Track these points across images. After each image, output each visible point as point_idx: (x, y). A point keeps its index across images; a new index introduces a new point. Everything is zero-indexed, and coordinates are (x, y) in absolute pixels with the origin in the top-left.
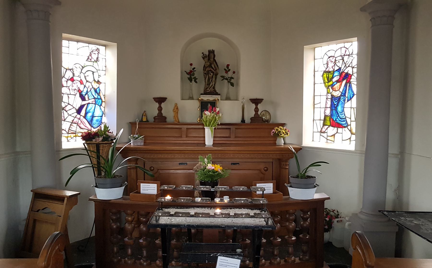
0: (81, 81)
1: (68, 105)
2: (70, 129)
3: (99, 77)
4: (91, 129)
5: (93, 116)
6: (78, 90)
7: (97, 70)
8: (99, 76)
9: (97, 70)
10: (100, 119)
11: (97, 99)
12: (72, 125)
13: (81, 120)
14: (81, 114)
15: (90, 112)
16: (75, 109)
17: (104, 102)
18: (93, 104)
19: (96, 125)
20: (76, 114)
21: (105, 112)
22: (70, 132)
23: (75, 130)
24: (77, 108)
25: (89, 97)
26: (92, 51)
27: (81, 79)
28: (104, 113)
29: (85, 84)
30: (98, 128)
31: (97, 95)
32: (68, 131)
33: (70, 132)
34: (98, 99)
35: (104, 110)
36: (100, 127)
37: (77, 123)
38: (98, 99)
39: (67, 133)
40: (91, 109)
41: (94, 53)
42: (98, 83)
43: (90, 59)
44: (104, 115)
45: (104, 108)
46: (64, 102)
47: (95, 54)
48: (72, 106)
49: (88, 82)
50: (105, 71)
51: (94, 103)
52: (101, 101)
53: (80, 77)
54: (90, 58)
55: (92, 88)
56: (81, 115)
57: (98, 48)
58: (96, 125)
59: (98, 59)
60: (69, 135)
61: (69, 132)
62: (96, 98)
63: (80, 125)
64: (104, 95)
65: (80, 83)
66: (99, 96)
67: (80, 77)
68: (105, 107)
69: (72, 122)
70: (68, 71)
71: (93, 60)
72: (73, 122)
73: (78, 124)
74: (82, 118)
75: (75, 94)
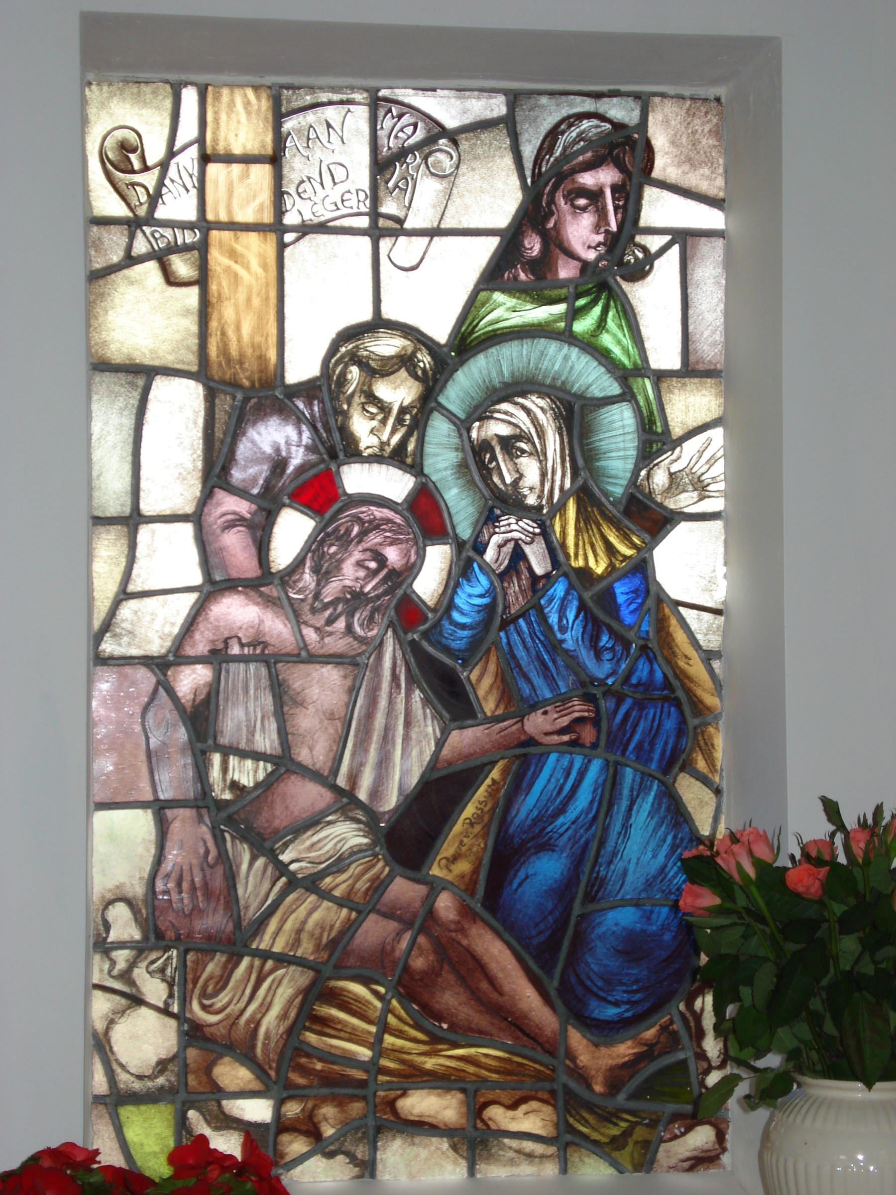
2: (311, 1038)
10: (667, 937)
14: (436, 871)
16: (360, 815)
19: (619, 996)
20: (380, 868)
24: (391, 801)
40: (562, 810)
41: (583, 192)
47: (595, 196)
54: (533, 245)
56: (435, 887)
60: (293, 1109)
67: (416, 468)
71: (566, 271)
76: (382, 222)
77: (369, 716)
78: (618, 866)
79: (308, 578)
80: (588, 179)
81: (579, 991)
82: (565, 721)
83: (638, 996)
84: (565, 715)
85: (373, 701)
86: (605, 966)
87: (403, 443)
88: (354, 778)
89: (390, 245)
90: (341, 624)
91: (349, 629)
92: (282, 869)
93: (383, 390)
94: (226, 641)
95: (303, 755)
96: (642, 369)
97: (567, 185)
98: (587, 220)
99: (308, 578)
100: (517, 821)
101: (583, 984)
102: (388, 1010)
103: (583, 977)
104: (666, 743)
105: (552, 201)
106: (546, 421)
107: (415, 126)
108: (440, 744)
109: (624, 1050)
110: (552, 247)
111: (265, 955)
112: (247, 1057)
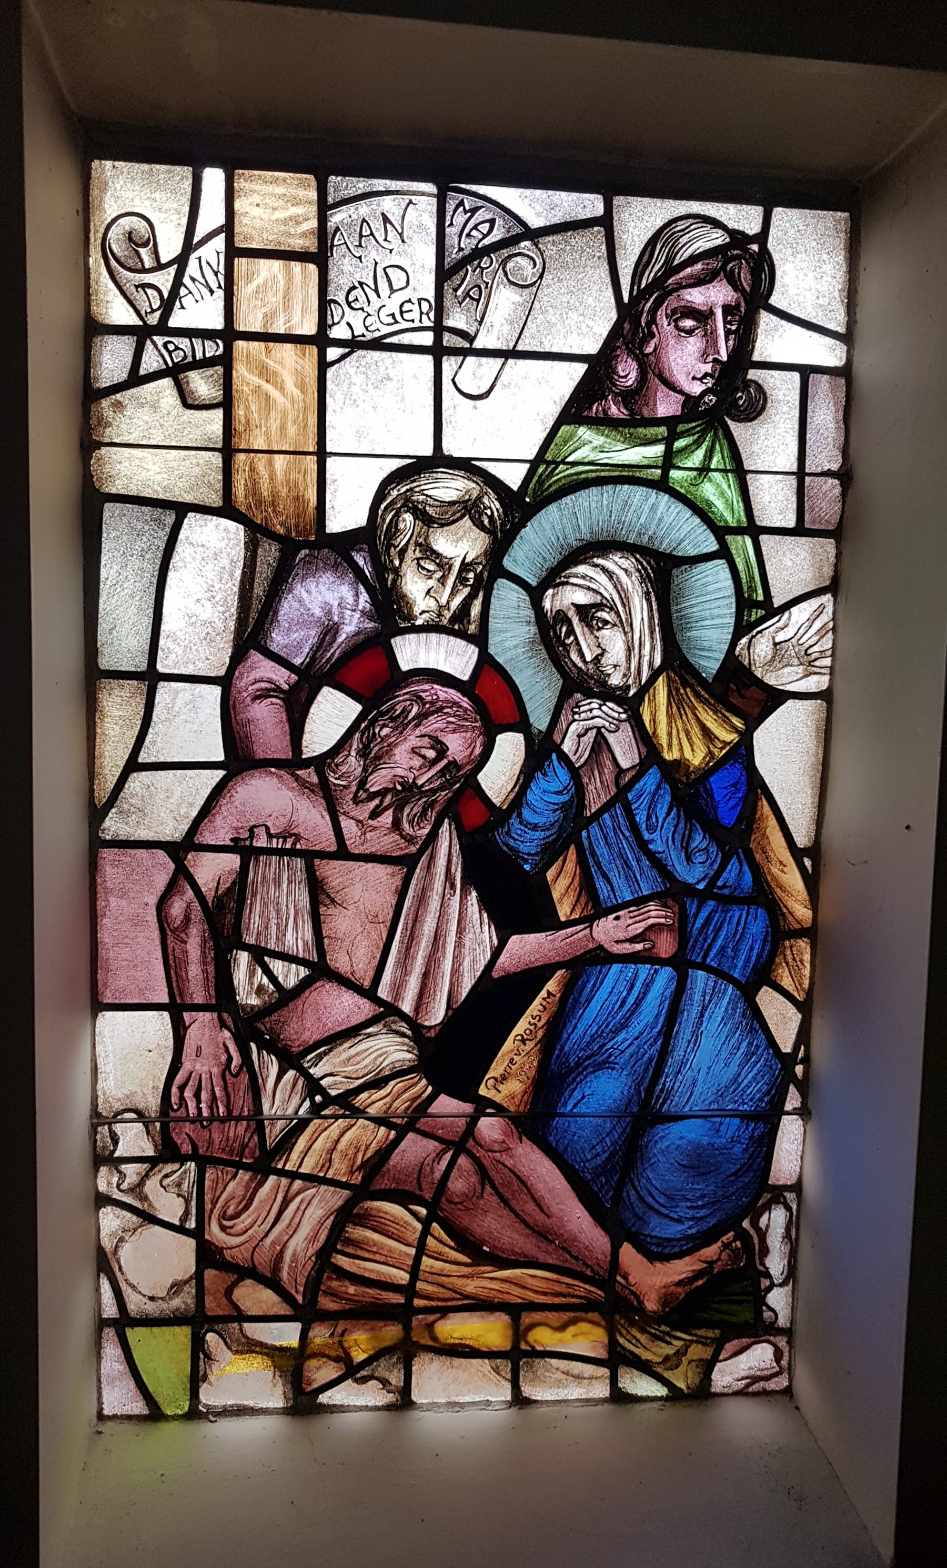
0: (490, 686)
1: (304, 985)
2: (342, 1261)
3: (742, 628)
4: (606, 1266)
5: (645, 1103)
6: (443, 795)
7: (720, 531)
8: (743, 602)
9: (720, 531)
10: (738, 1149)
11: (702, 897)
12: (365, 1220)
13: (479, 1153)
15: (600, 1066)
16: (404, 1027)
17: (810, 933)
18: (644, 970)
20: (422, 1086)
21: (806, 1061)
22: (334, 1295)
23: (402, 1277)
24: (437, 1014)
25: (601, 884)
26: (658, 282)
27: (486, 662)
28: (799, 1069)
29: (540, 720)
30: (711, 1252)
31: (713, 849)
32: (313, 1286)
33: (334, 1295)
34: (720, 899)
35: (804, 1035)
36: (742, 1235)
37: (428, 1196)
38: (729, 900)
39: (284, 1309)
41: (690, 312)
42: (735, 700)
43: (629, 397)
44: (793, 1100)
45: (804, 1007)
46: (259, 955)
47: (703, 317)
48: (370, 993)
49: (589, 694)
50: (836, 534)
51: (666, 946)
52: (758, 925)
53: (480, 639)
55: (641, 769)
56: (483, 1106)
57: (738, 238)
58: (682, 1210)
59: (747, 384)
60: (320, 1335)
61: (327, 1303)
62: (689, 890)
63: (465, 1221)
64: (802, 839)
65: (465, 702)
66: (733, 866)
67: (480, 639)
68: (810, 993)
69: (357, 1179)
70: (307, 562)
72: (383, 1183)
73: (444, 1204)
74: (489, 1127)
75: (413, 849)
76: (449, 340)
77: (416, 920)
78: (687, 1075)
79: (352, 764)
80: (696, 297)
81: (639, 1208)
82: (639, 928)
83: (703, 1212)
84: (640, 921)
85: (422, 899)
86: (668, 1182)
87: (466, 605)
88: (398, 988)
89: (455, 367)
90: (387, 818)
91: (396, 825)
92: (313, 1086)
93: (443, 543)
94: (251, 830)
95: (339, 961)
96: (754, 530)
97: (672, 302)
98: (694, 344)
99: (352, 764)
100: (580, 1030)
101: (641, 1199)
102: (426, 1232)
103: (644, 1193)
104: (752, 948)
105: (652, 321)
106: (633, 586)
107: (492, 222)
108: (497, 953)
109: (682, 1268)
110: (651, 375)
111: (294, 1176)
112: (273, 1282)
